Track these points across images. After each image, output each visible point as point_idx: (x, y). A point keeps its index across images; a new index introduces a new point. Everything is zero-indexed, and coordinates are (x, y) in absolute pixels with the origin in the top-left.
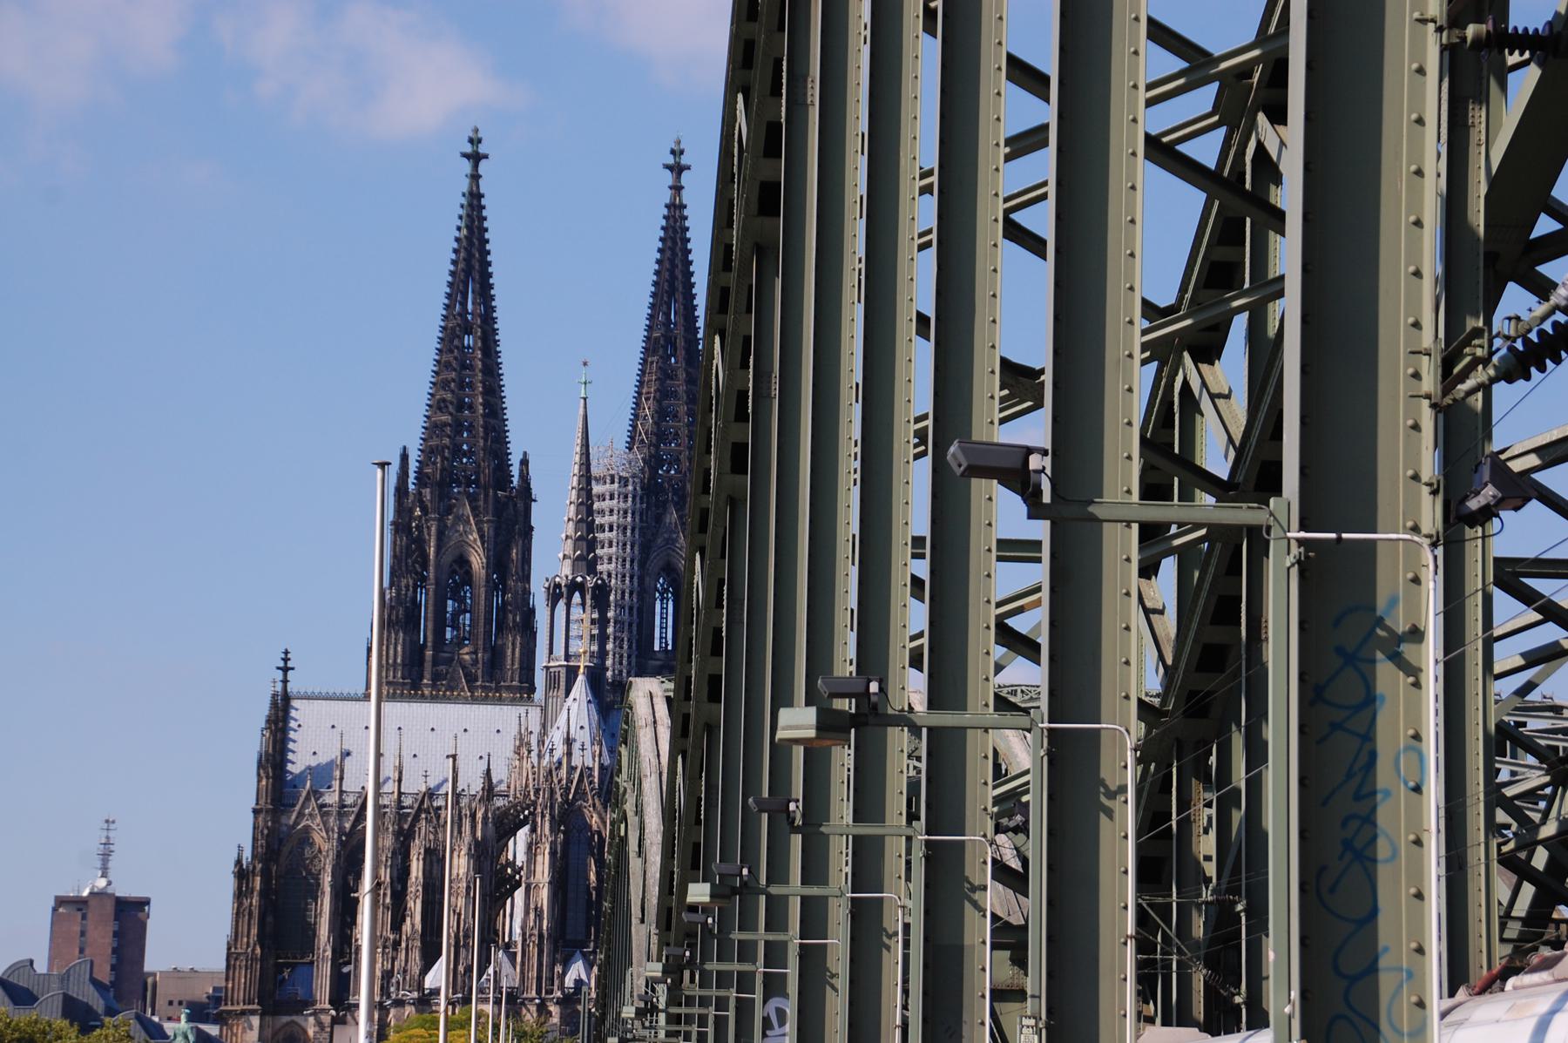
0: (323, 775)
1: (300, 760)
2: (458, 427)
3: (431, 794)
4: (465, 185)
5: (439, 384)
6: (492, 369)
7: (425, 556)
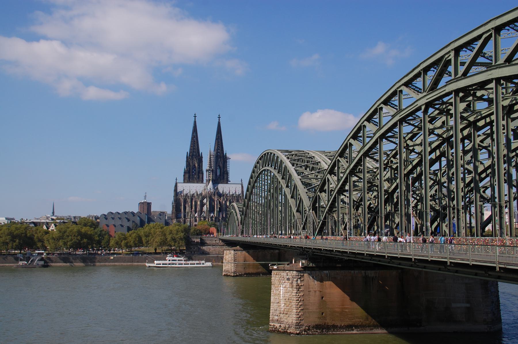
0: (181, 192)
1: (178, 191)
2: (194, 149)
3: (193, 194)
6: (198, 142)
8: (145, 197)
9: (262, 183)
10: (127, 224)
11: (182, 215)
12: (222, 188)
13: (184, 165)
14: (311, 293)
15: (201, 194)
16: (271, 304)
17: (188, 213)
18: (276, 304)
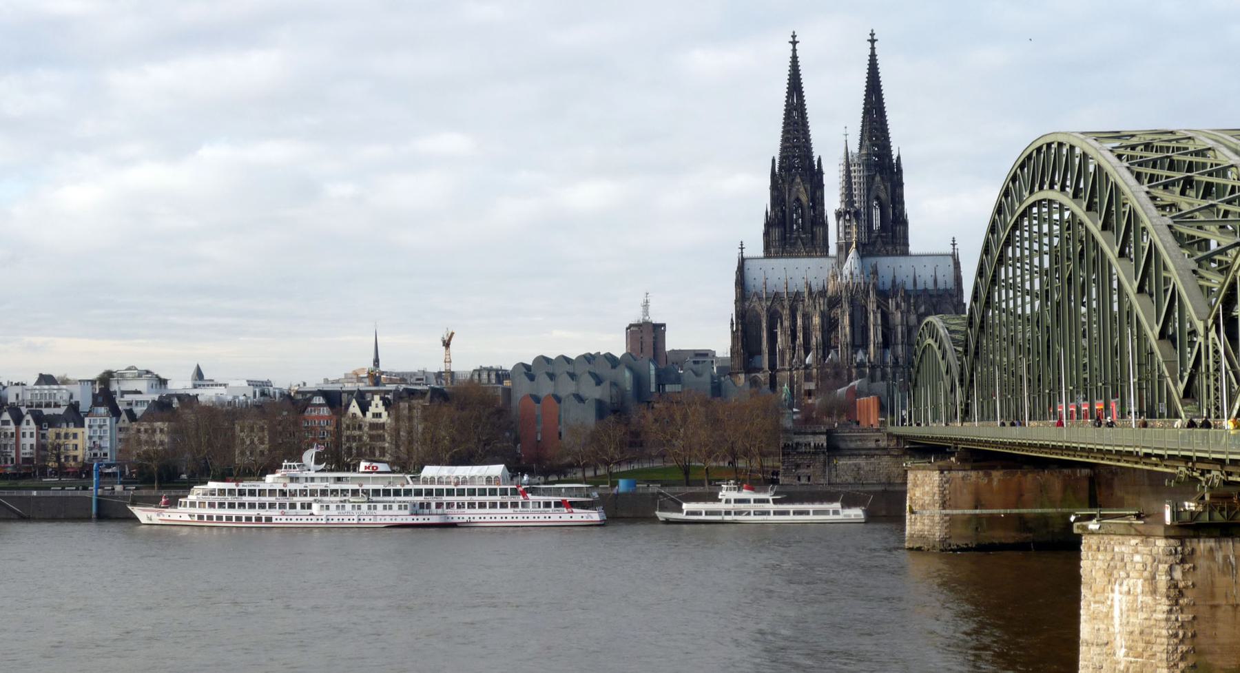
4: (791, 54)
5: (786, 131)
7: (784, 200)
8: (646, 305)
9: (1031, 248)
10: (593, 392)
11: (766, 365)
12: (889, 266)
13: (763, 201)
14: (1220, 614)
15: (823, 293)
16: (1083, 649)
17: (783, 353)
18: (1098, 650)
